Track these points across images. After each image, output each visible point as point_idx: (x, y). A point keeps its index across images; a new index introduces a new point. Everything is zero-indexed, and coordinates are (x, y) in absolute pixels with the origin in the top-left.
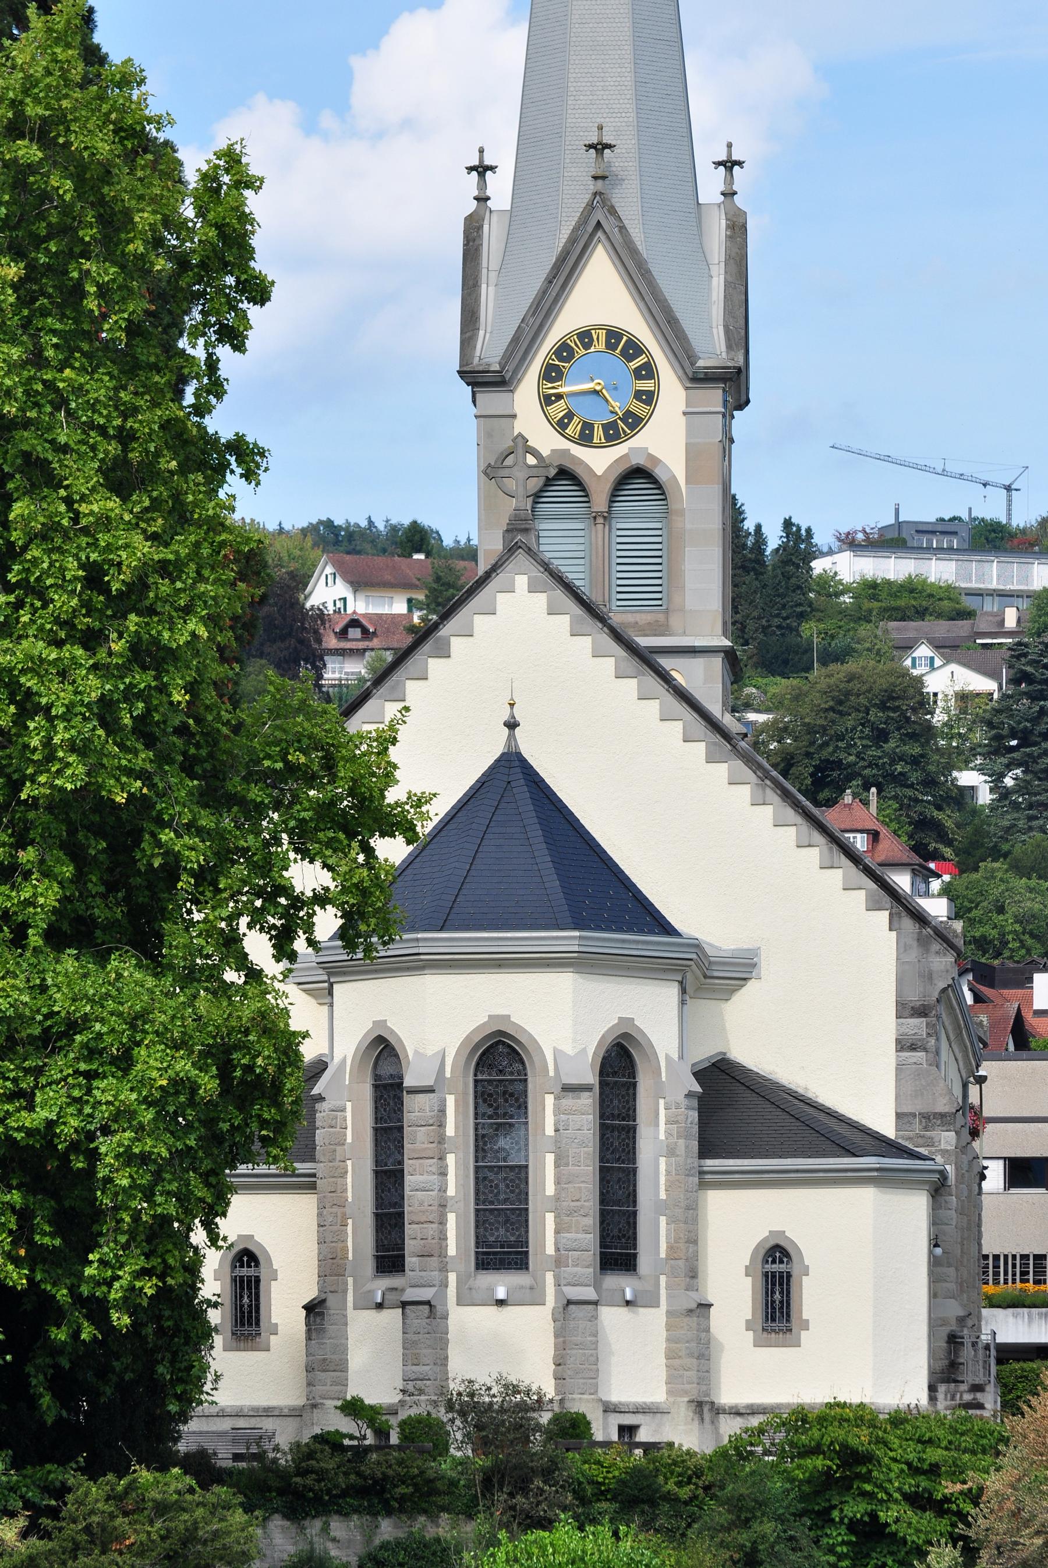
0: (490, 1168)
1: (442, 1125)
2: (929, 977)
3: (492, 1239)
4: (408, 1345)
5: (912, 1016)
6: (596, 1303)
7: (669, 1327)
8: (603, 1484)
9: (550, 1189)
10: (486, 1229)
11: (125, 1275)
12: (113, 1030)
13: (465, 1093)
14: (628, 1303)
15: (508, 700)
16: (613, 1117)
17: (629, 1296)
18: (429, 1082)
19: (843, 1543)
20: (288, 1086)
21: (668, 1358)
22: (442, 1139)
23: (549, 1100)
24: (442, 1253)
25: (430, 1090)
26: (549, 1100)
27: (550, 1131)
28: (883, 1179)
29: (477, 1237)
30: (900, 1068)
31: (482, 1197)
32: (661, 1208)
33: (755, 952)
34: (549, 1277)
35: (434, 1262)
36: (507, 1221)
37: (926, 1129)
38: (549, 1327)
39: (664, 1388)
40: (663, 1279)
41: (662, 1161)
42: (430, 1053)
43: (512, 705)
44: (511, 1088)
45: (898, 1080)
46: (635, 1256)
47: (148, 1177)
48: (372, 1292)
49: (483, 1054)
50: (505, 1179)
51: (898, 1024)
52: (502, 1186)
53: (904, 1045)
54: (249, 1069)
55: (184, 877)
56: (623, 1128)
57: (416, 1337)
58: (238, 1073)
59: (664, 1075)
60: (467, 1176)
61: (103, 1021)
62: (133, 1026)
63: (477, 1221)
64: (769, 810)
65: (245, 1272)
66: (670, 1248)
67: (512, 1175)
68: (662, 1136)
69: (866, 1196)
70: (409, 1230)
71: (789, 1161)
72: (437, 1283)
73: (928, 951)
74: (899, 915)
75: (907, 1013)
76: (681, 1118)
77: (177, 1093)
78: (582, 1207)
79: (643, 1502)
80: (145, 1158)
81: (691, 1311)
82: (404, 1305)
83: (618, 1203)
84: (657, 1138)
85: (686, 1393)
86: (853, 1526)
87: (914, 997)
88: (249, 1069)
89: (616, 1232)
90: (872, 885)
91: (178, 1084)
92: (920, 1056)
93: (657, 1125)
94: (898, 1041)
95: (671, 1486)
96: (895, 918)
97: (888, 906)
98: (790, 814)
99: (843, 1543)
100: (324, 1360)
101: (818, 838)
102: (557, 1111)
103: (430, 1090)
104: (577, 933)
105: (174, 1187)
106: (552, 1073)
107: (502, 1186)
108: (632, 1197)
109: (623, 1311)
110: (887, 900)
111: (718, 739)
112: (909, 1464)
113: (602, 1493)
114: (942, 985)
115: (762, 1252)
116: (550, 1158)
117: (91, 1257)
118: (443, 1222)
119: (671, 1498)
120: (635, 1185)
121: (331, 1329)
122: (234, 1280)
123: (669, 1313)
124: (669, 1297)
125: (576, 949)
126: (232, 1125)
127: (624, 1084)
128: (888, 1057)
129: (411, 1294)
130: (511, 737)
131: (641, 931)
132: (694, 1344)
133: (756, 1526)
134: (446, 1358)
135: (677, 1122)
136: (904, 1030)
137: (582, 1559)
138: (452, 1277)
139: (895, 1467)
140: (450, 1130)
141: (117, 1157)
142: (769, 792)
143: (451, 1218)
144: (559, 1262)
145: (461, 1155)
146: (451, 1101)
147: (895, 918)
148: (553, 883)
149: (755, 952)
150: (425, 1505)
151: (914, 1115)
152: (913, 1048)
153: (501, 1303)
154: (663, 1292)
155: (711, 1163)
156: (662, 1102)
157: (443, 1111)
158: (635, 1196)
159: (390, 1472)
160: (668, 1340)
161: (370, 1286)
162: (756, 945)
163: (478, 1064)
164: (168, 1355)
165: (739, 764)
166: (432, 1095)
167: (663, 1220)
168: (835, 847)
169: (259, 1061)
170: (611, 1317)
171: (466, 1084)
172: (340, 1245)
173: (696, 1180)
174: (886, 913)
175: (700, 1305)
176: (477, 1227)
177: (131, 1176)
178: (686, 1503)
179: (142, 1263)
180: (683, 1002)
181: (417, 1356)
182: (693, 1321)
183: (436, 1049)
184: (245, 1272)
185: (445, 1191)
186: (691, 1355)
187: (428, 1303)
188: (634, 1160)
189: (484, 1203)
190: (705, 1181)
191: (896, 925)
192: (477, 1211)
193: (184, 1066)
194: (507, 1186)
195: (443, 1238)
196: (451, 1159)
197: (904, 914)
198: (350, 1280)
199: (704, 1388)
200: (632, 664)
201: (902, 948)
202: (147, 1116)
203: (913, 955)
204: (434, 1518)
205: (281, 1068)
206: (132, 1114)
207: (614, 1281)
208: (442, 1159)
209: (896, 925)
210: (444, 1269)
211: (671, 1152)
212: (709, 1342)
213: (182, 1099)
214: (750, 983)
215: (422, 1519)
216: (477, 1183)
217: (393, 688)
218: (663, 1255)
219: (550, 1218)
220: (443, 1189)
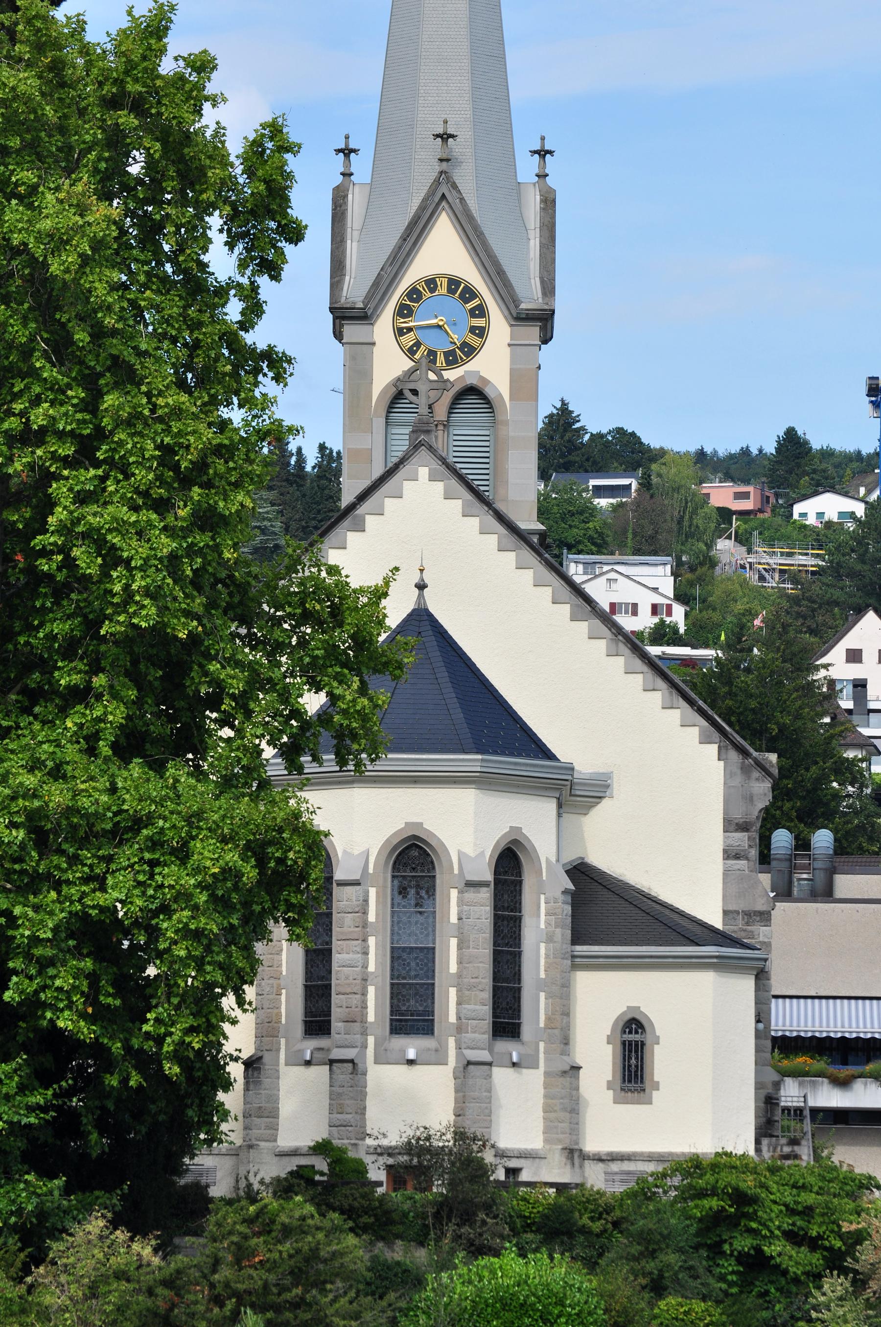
1: (365, 913)
2: (750, 799)
3: (404, 1008)
4: (333, 1096)
5: (736, 831)
6: (490, 1064)
8: (529, 1218)
9: (453, 968)
10: (399, 1000)
11: (177, 1031)
12: (174, 826)
13: (385, 887)
14: (514, 1065)
15: (418, 566)
17: (515, 1059)
18: (356, 876)
19: (733, 1272)
20: (313, 876)
21: (545, 1111)
22: (365, 924)
24: (364, 1020)
25: (356, 883)
26: (454, 894)
27: (454, 919)
28: (721, 965)
29: (392, 1007)
30: (726, 873)
31: (396, 973)
32: (541, 985)
33: (609, 775)
34: (452, 1042)
35: (356, 1026)
36: (416, 994)
37: (748, 924)
38: (451, 1083)
40: (542, 1045)
42: (356, 852)
43: (422, 571)
45: (725, 883)
46: (519, 1025)
47: (201, 949)
48: (302, 1051)
49: (400, 854)
50: (416, 958)
51: (725, 837)
52: (413, 964)
53: (730, 854)
54: (281, 861)
55: (227, 701)
57: (340, 1090)
58: (272, 864)
59: (544, 874)
60: (385, 955)
61: (165, 819)
62: (190, 824)
63: (392, 993)
66: (548, 1019)
67: (421, 955)
68: (543, 926)
69: (707, 978)
70: (335, 999)
71: (644, 948)
72: (359, 1044)
73: (749, 778)
74: (726, 747)
75: (732, 828)
76: (559, 911)
77: (225, 880)
78: (480, 983)
79: (563, 1234)
80: (197, 935)
81: (565, 1072)
82: (331, 1062)
84: (538, 926)
85: (560, 1141)
86: (741, 1258)
87: (738, 815)
88: (281, 861)
89: (504, 1005)
90: (704, 723)
91: (228, 872)
92: (743, 863)
93: (539, 916)
94: (725, 851)
95: (585, 1220)
96: (723, 751)
97: (718, 740)
99: (733, 1272)
100: (260, 1108)
101: (661, 683)
102: (461, 902)
103: (356, 883)
104: (479, 757)
105: (221, 958)
106: (456, 871)
107: (413, 964)
109: (510, 1071)
110: (716, 735)
111: (580, 602)
112: (786, 1205)
113: (529, 1225)
115: (621, 1024)
116: (454, 942)
117: (149, 1016)
118: (364, 994)
119: (584, 1231)
120: (520, 966)
121: (266, 1082)
123: (547, 1074)
124: (547, 1060)
125: (479, 769)
126: (263, 908)
127: (513, 882)
128: (716, 864)
129: (337, 1054)
130: (421, 597)
131: (528, 756)
132: (566, 1101)
133: (662, 1257)
134: (365, 1108)
135: (555, 914)
136: (730, 842)
137: (526, 1282)
138: (371, 1040)
139: (776, 1208)
140: (372, 917)
141: (177, 932)
143: (371, 990)
144: (460, 1029)
145: (380, 938)
146: (373, 892)
147: (723, 751)
148: (458, 715)
149: (609, 775)
150: (383, 1233)
151: (737, 912)
152: (737, 857)
153: (411, 1062)
154: (542, 1056)
155: (580, 949)
156: (542, 897)
157: (366, 901)
158: (520, 975)
159: (356, 1204)
160: (546, 1096)
161: (299, 1046)
162: (610, 770)
163: (395, 863)
164: (197, 1101)
165: (597, 622)
166: (358, 888)
167: (542, 995)
168: (674, 692)
169: (291, 855)
170: (501, 1075)
172: (276, 1011)
173: (569, 962)
174: (716, 746)
177: (187, 948)
178: (598, 1236)
179: (191, 1021)
180: (559, 815)
181: (341, 1106)
182: (566, 1081)
183: (362, 849)
186: (564, 1109)
187: (352, 1061)
188: (519, 945)
189: (398, 978)
190: (577, 964)
191: (724, 756)
192: (392, 985)
193: (232, 857)
194: (417, 964)
196: (372, 941)
197: (730, 747)
198: (283, 1041)
199: (574, 1137)
201: (728, 775)
202: (202, 898)
203: (738, 780)
204: (390, 1244)
205: (307, 862)
206: (188, 896)
207: (504, 1046)
208: (365, 940)
209: (724, 756)
211: (549, 939)
213: (229, 884)
215: (380, 1245)
216: (392, 962)
218: (542, 1025)
219: (453, 992)
220: (365, 966)
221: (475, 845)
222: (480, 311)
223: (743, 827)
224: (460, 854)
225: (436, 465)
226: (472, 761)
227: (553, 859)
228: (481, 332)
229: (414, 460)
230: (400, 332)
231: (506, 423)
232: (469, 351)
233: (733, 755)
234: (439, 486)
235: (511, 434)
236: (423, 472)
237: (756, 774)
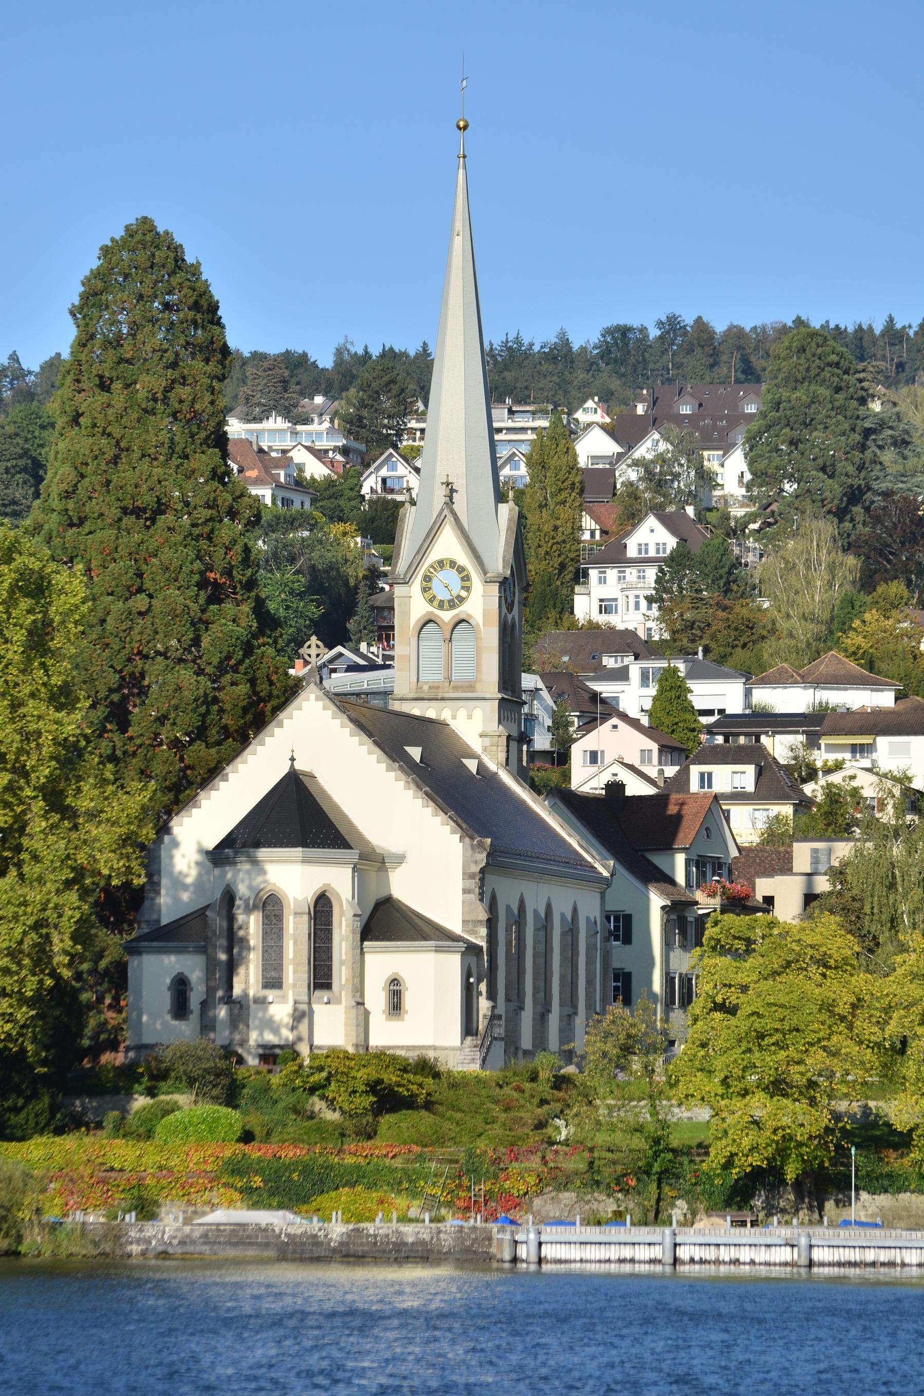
9: (291, 956)
23: (291, 918)
26: (291, 918)
28: (438, 950)
32: (342, 963)
40: (343, 993)
41: (344, 943)
53: (465, 891)
65: (182, 987)
108: (330, 958)
111: (390, 762)
116: (291, 943)
128: (459, 897)
130: (292, 765)
144: (294, 986)
184: (182, 987)
200: (358, 730)
201: (464, 850)
203: (470, 852)
207: (318, 993)
218: (343, 982)
219: (291, 968)
222: (467, 578)
224: (295, 899)
226: (298, 852)
228: (468, 589)
229: (308, 690)
230: (425, 590)
231: (481, 639)
232: (461, 600)
234: (320, 704)
236: (312, 696)
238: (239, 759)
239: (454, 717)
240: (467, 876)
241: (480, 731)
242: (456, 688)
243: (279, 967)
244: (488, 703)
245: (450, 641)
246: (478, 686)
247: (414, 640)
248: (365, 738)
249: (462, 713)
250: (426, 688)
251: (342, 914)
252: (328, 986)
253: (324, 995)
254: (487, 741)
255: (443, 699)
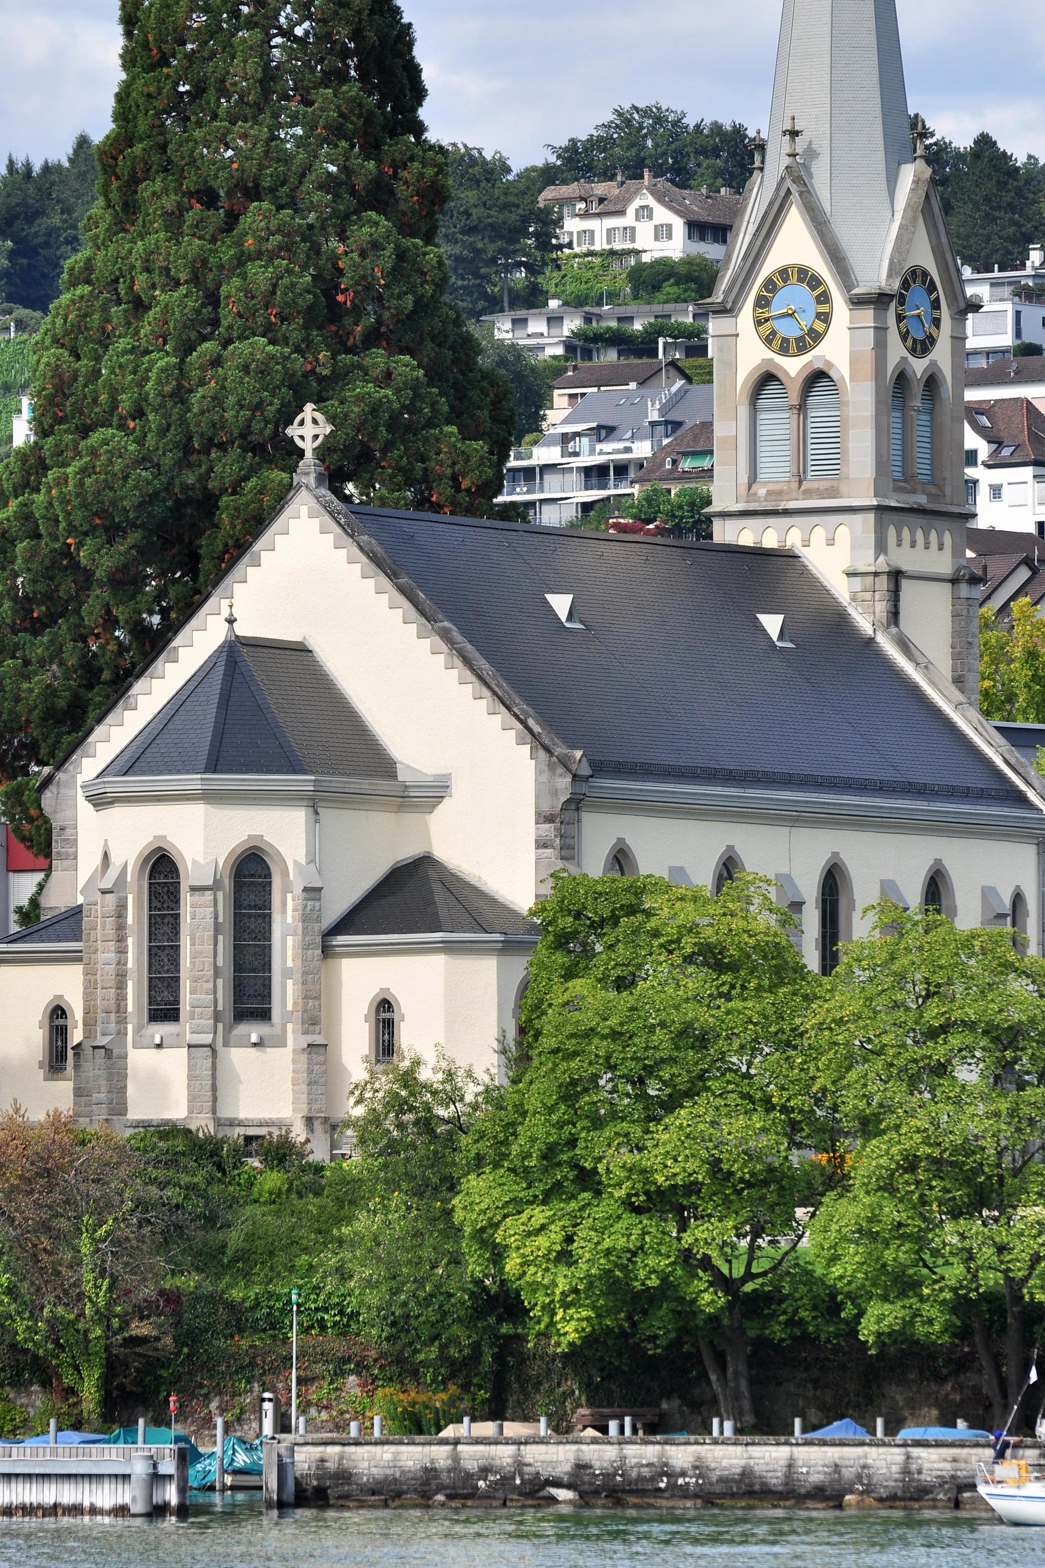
0: (159, 947)
2: (555, 793)
5: (544, 822)
7: (294, 1061)
14: (255, 1045)
16: (250, 907)
22: (121, 927)
30: (538, 860)
32: (287, 974)
33: (448, 776)
39: (291, 1107)
40: (290, 1026)
44: (172, 889)
51: (537, 829)
53: (541, 844)
56: (260, 915)
64: (455, 672)
66: (295, 1003)
68: (289, 920)
69: (439, 960)
73: (554, 774)
75: (542, 820)
76: (300, 907)
83: (254, 970)
84: (284, 921)
87: (546, 809)
89: (251, 992)
90: (520, 726)
92: (548, 852)
98: (468, 675)
101: (486, 692)
104: (199, 776)
108: (267, 966)
111: (424, 621)
114: (563, 799)
115: (375, 1004)
118: (121, 986)
122: (51, 1027)
124: (295, 1039)
127: (260, 884)
128: (529, 853)
134: (125, 1087)
138: (130, 1027)
140: (130, 920)
142: (456, 659)
146: (130, 897)
149: (448, 776)
152: (545, 846)
153: (159, 1046)
156: (289, 896)
157: (122, 907)
171: (140, 887)
175: (309, 1045)
176: (150, 990)
180: (317, 821)
183: (123, 861)
185: (125, 964)
187: (103, 1047)
195: (121, 998)
196: (130, 941)
200: (372, 568)
201: (539, 772)
208: (121, 939)
210: (122, 1021)
212: (325, 1072)
214: (446, 800)
216: (150, 959)
217: (225, 589)
218: (290, 1008)
220: (121, 963)
221: (206, 853)
223: (549, 819)
224: (194, 861)
225: (313, 502)
226: (193, 781)
227: (303, 861)
233: (542, 754)
235: (851, 414)
236: (304, 510)
237: (560, 770)
238: (194, 623)
239: (806, 544)
240: (544, 818)
241: (846, 564)
242: (809, 494)
243: (173, 984)
244: (859, 518)
245: (802, 408)
246: (843, 487)
247: (743, 411)
248: (384, 580)
249: (819, 535)
250: (762, 492)
251: (286, 889)
252: (264, 1015)
253: (254, 1031)
254: (857, 583)
255: (787, 513)
